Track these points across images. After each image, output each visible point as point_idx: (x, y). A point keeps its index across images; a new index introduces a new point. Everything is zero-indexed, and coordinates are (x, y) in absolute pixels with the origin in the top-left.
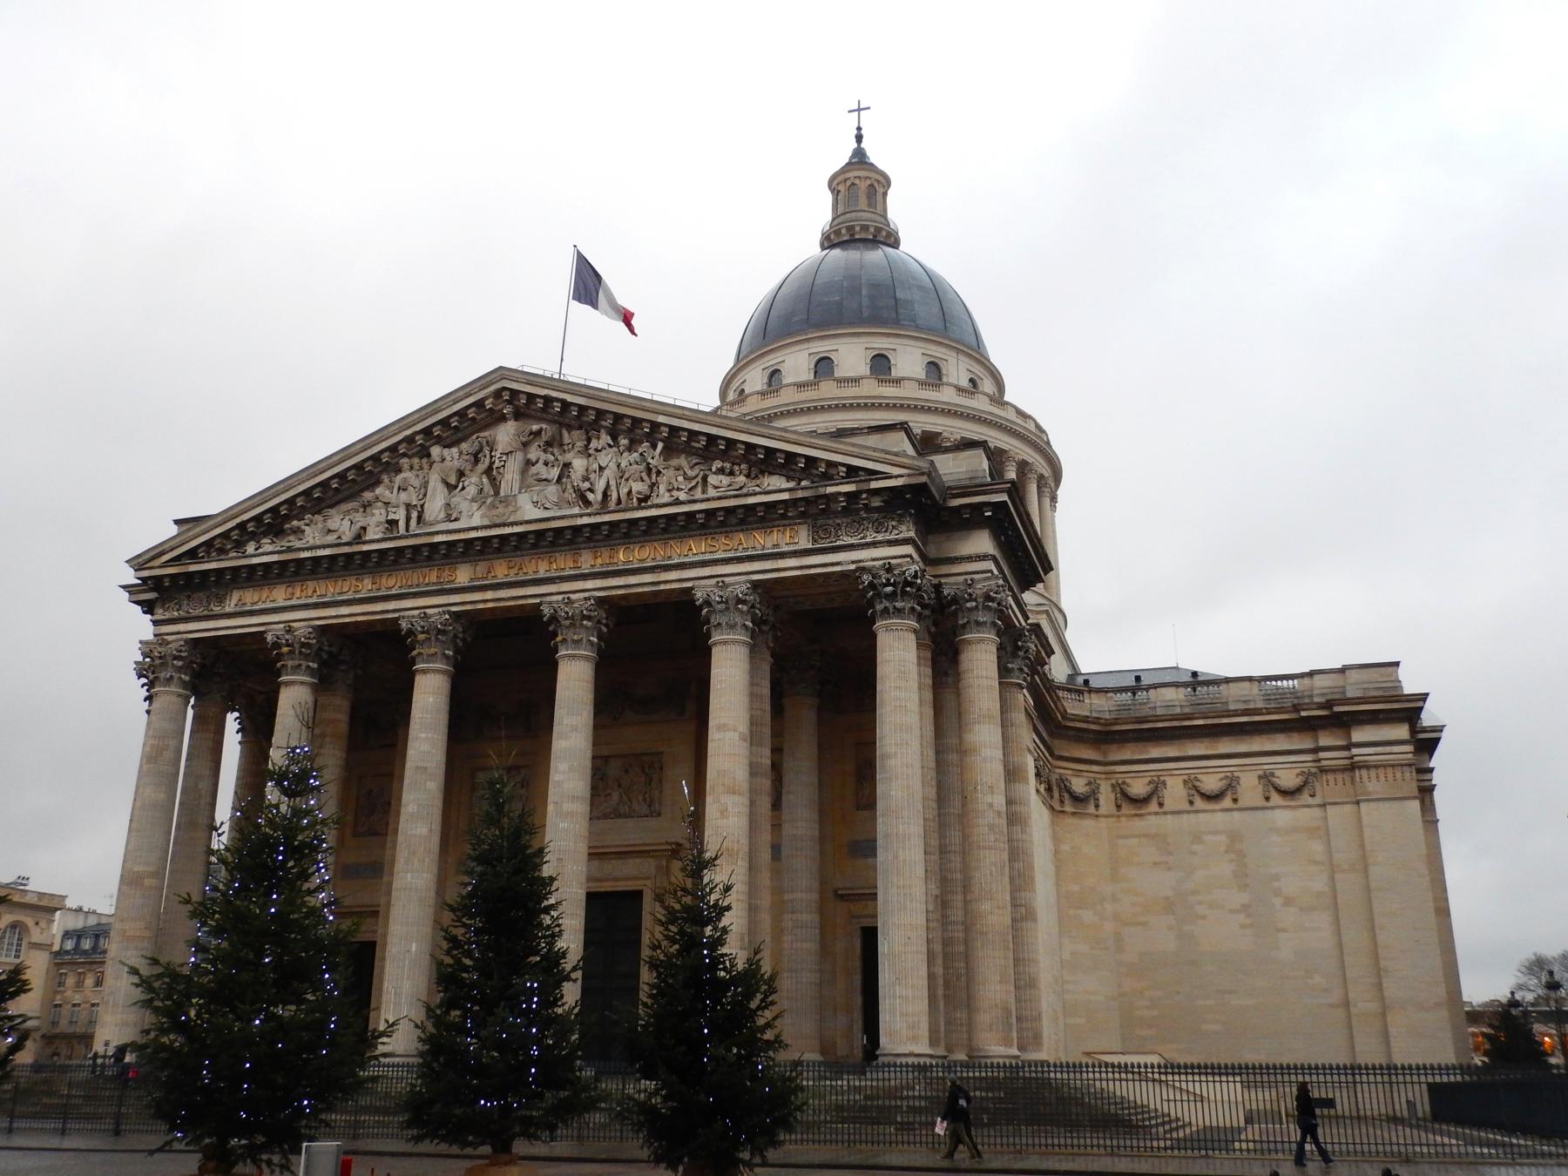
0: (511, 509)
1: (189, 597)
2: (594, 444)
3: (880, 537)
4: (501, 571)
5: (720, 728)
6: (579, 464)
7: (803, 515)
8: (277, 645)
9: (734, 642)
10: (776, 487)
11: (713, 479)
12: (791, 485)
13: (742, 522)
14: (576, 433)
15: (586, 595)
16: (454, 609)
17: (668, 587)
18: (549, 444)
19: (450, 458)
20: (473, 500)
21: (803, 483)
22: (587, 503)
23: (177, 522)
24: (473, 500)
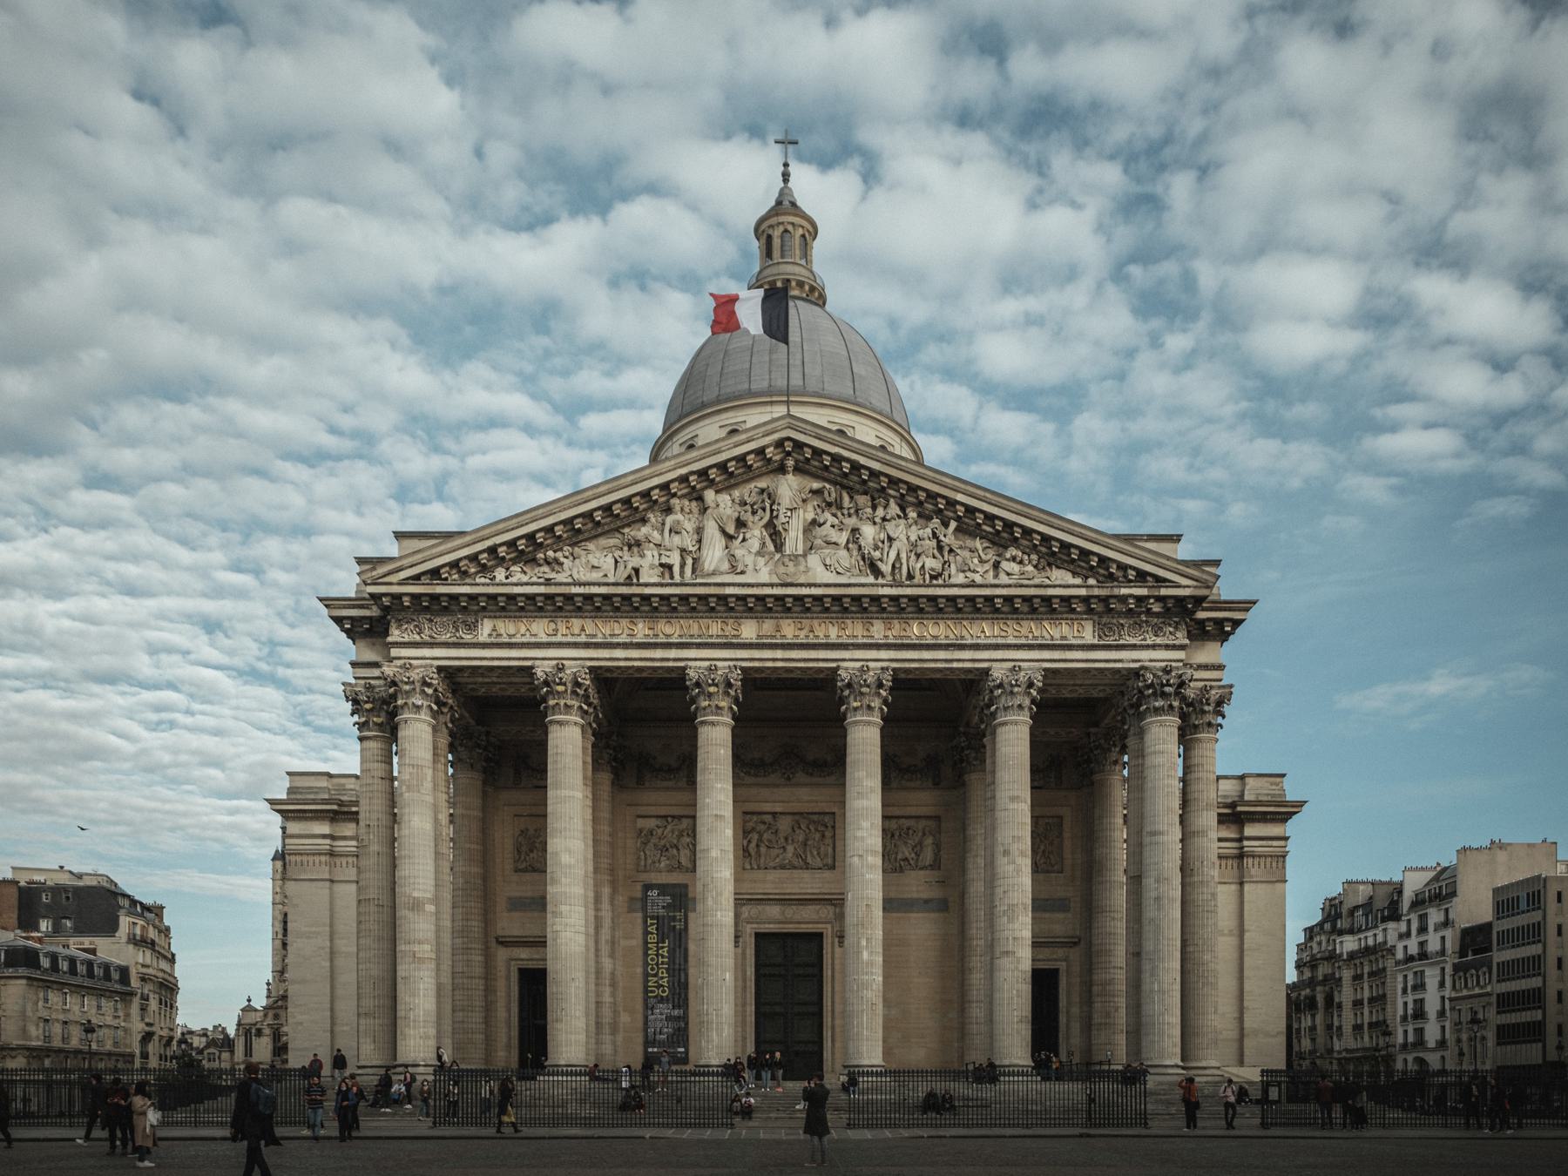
0: (802, 568)
1: (431, 621)
2: (880, 512)
3: (1159, 641)
4: (789, 630)
5: (1013, 799)
6: (869, 532)
7: (1090, 611)
8: (546, 683)
9: (1025, 722)
10: (1062, 581)
11: (1005, 565)
12: (1078, 581)
13: (1034, 610)
14: (863, 500)
15: (885, 664)
16: (745, 664)
17: (960, 665)
18: (829, 505)
19: (723, 504)
20: (759, 553)
21: (1092, 581)
22: (877, 572)
23: (400, 536)
24: (759, 553)
